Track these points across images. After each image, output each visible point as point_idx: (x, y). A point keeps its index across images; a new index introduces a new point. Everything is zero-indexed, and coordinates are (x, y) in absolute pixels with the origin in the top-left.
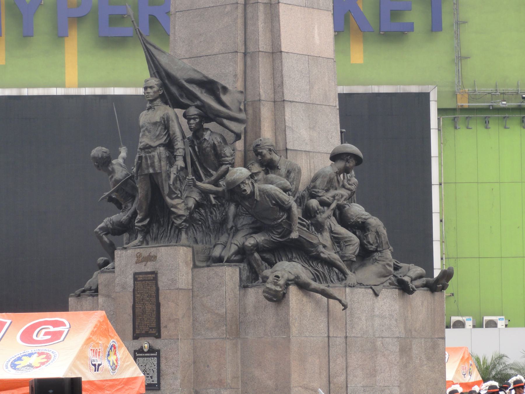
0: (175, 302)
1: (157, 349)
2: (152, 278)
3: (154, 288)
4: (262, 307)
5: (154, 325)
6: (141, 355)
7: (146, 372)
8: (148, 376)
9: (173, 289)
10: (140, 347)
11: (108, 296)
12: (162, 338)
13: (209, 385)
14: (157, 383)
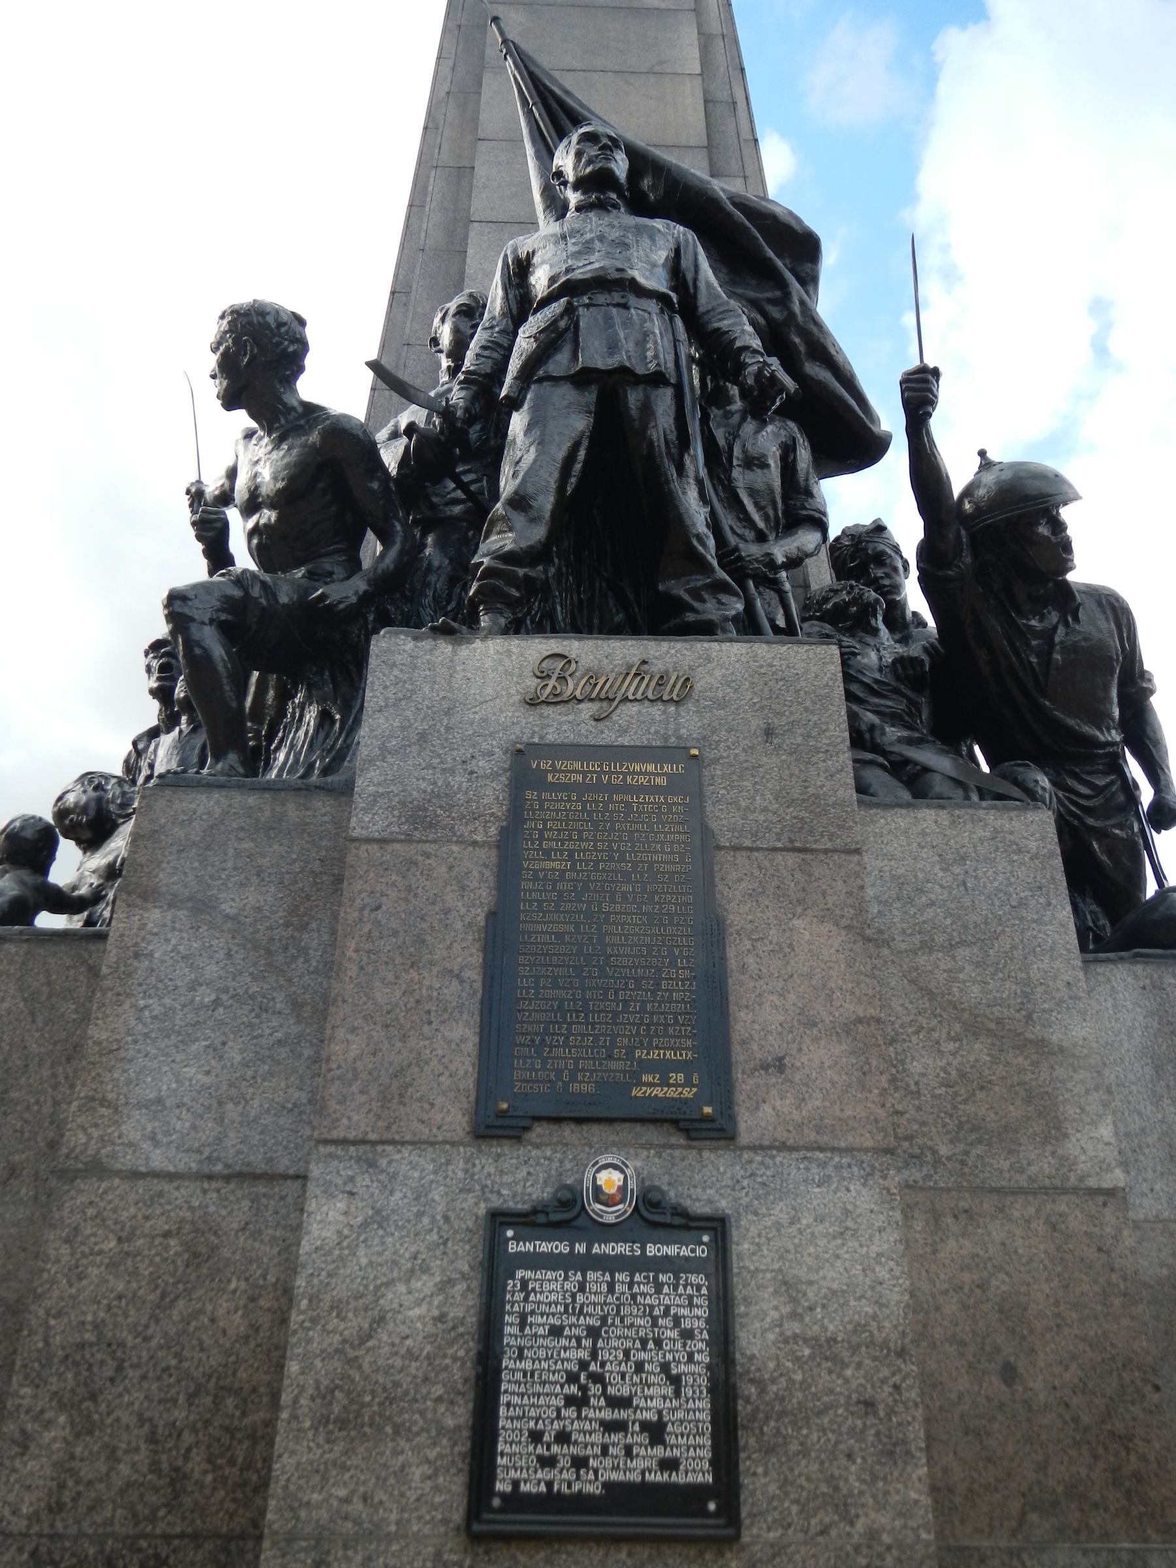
0: (844, 922)
1: (699, 1208)
7: (595, 1389)
8: (623, 1414)
9: (826, 851)
13: (1034, 1517)
14: (709, 1478)
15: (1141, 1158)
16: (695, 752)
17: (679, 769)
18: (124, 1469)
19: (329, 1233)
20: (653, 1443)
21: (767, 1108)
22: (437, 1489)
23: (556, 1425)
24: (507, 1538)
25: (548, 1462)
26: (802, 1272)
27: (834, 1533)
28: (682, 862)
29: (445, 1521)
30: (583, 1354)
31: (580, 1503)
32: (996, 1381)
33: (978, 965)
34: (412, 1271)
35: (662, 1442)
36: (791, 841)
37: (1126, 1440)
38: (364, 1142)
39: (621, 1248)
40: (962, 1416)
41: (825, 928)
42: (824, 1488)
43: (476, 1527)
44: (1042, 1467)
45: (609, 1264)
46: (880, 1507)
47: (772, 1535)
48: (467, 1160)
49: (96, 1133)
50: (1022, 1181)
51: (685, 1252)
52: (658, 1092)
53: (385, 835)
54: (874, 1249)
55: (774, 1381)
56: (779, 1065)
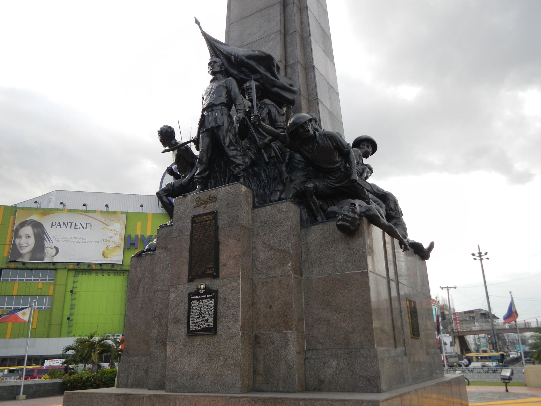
1: (215, 289)
2: (211, 218)
4: (329, 243)
6: (197, 297)
7: (201, 316)
8: (204, 319)
9: (234, 226)
10: (195, 290)
12: (220, 277)
13: (272, 328)
15: (315, 264)
16: (216, 211)
17: (213, 215)
18: (164, 330)
20: (207, 322)
21: (223, 272)
22: (184, 330)
23: (196, 321)
24: (192, 335)
25: (195, 326)
26: (226, 297)
27: (228, 332)
28: (213, 233)
29: (186, 334)
30: (199, 311)
31: (199, 331)
32: (269, 308)
33: (273, 236)
34: (181, 302)
35: (208, 322)
36: (229, 225)
37: (286, 316)
38: (175, 285)
39: (204, 296)
40: (263, 314)
42: (227, 327)
43: (188, 334)
44: (274, 321)
45: (203, 299)
46: (233, 329)
47: (221, 333)
48: (187, 286)
50: (276, 275)
51: (211, 296)
52: (209, 272)
54: (236, 292)
55: (222, 313)
56: (225, 265)
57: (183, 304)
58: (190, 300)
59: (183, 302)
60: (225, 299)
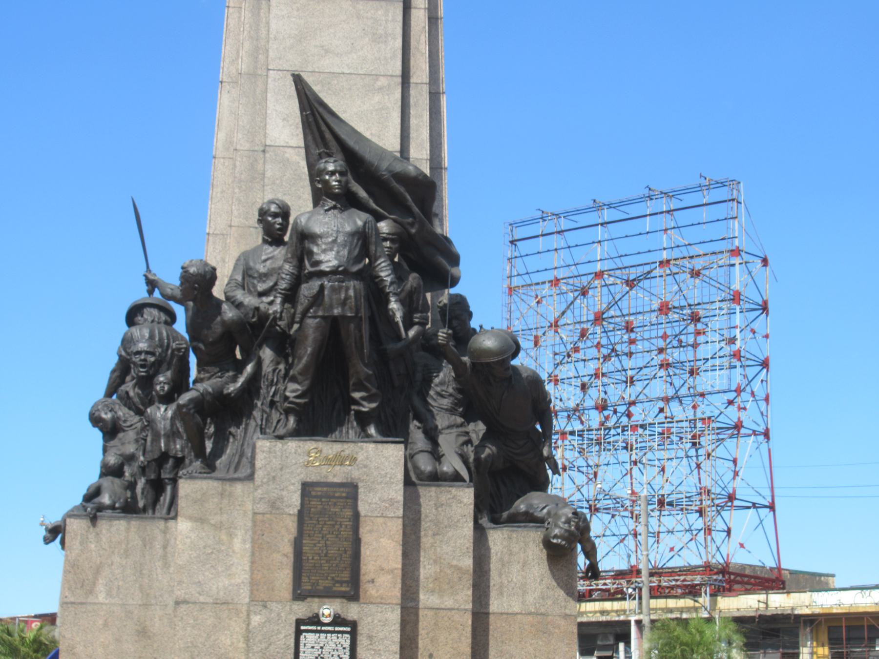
3: (348, 513)
5: (346, 575)
6: (314, 628)
9: (392, 517)
11: (201, 520)
12: (361, 600)
19: (256, 624)
26: (374, 635)
30: (320, 653)
39: (330, 628)
41: (389, 542)
49: (183, 591)
53: (264, 511)
56: (373, 581)
57: (281, 636)
58: (298, 633)
59: (280, 633)
60: (370, 637)
